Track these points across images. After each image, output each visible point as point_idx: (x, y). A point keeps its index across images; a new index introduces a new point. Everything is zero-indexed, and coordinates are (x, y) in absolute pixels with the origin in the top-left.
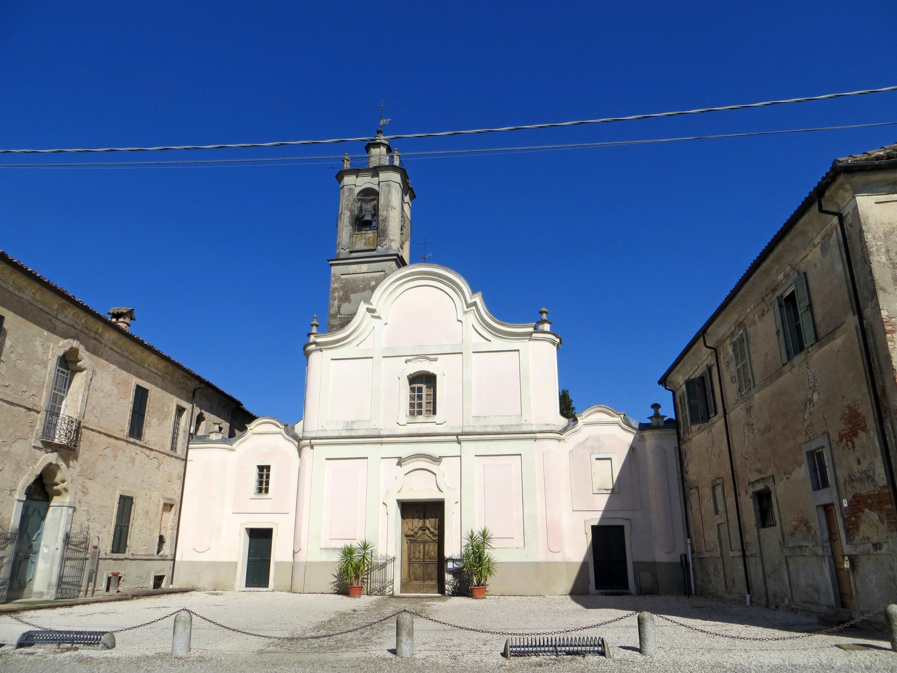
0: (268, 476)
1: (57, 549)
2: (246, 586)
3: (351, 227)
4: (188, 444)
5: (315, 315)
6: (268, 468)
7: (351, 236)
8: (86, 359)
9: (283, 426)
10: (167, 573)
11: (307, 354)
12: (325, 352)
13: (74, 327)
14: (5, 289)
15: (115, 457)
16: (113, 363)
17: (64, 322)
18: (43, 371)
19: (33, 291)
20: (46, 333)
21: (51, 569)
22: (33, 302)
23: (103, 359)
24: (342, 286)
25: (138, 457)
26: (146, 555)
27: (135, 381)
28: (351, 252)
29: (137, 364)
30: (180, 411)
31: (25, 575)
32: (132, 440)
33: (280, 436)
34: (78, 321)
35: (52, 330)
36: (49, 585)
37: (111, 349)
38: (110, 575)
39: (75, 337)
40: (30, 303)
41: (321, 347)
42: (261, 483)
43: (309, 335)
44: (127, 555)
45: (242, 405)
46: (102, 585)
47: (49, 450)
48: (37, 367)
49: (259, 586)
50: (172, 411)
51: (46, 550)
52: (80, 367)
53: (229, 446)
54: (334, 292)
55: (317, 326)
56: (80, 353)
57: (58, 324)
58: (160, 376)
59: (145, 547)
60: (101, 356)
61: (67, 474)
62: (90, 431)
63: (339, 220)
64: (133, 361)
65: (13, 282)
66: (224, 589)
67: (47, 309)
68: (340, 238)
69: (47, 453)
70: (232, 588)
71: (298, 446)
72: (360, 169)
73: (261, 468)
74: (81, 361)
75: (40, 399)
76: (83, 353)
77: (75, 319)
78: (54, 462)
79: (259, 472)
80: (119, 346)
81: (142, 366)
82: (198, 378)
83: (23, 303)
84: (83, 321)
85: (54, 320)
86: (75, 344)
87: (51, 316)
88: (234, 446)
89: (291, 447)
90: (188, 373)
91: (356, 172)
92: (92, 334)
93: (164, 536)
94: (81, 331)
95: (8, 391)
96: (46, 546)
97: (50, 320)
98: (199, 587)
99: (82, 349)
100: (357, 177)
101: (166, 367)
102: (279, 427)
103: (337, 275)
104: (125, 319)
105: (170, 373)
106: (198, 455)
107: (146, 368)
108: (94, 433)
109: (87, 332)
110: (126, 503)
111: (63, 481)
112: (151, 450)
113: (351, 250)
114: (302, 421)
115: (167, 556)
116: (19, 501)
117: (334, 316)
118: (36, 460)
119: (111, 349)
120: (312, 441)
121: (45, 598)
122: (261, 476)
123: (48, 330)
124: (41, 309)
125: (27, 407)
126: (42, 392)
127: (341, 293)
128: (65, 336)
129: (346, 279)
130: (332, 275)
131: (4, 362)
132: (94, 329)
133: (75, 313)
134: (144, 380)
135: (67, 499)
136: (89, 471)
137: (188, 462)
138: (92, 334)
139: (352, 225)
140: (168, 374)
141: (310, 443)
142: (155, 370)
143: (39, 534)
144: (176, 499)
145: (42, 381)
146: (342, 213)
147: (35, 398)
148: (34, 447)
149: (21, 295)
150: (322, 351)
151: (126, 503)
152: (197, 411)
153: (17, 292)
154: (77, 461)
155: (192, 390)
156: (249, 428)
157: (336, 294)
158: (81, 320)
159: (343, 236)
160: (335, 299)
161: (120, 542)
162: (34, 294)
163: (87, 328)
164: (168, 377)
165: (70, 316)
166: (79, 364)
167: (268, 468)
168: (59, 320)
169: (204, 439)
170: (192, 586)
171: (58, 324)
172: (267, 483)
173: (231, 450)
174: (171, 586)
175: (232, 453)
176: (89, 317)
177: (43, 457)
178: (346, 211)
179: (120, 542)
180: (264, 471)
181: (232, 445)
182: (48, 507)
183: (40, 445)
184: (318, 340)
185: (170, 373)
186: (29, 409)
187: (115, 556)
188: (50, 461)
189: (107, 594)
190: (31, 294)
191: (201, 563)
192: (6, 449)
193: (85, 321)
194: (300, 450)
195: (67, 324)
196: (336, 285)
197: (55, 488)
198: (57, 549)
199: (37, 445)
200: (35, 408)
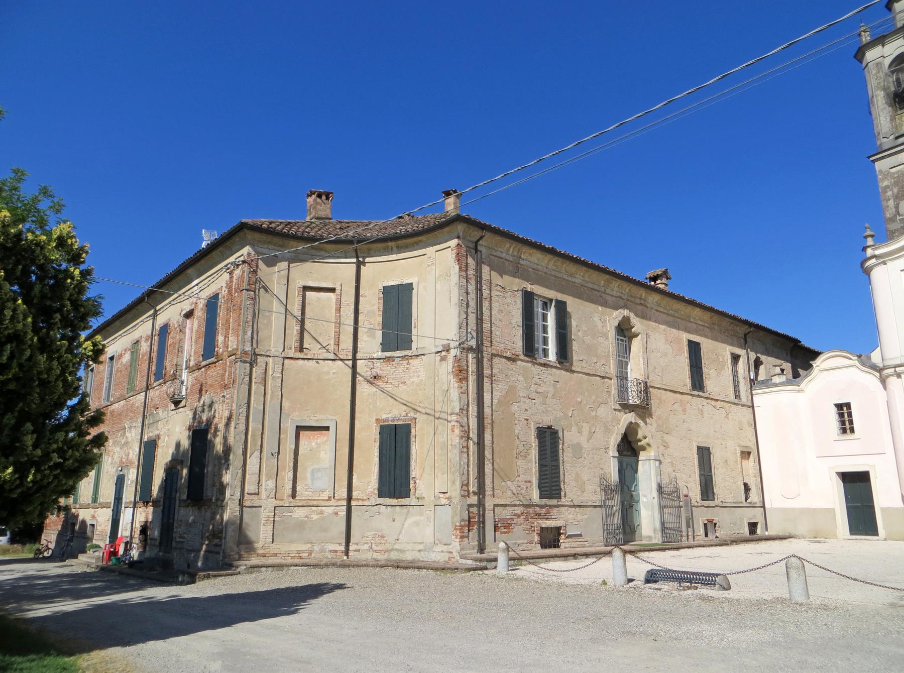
0: (850, 415)
1: (654, 498)
2: (851, 534)
3: (890, 108)
4: (751, 391)
5: (867, 225)
6: (848, 405)
7: (893, 119)
8: (638, 325)
9: (856, 358)
10: (759, 519)
11: (867, 272)
12: (889, 264)
13: (621, 298)
14: (560, 278)
15: (684, 411)
16: (662, 324)
17: (612, 296)
18: (606, 342)
19: (582, 274)
20: (600, 308)
21: (653, 516)
23: (652, 321)
24: (894, 182)
25: (705, 409)
26: (735, 503)
27: (685, 337)
28: (897, 138)
30: (735, 358)
31: (633, 521)
32: (696, 393)
33: (854, 368)
34: (623, 292)
35: (605, 304)
36: (655, 530)
37: (657, 311)
38: (706, 522)
39: (625, 307)
40: (582, 285)
41: (883, 259)
42: (843, 423)
43: (864, 249)
44: (716, 502)
45: (800, 342)
46: (700, 531)
47: (627, 411)
48: (601, 340)
49: (867, 534)
50: (727, 359)
51: (645, 500)
52: (634, 333)
53: (796, 388)
54: (886, 192)
55: (872, 236)
56: (632, 320)
57: (608, 298)
58: (707, 327)
59: (732, 495)
60: (650, 320)
61: (646, 431)
63: (871, 106)
64: (679, 318)
65: (565, 271)
66: (826, 537)
67: (596, 287)
68: (878, 126)
69: (626, 413)
70: (835, 536)
71: (881, 377)
72: (885, 34)
73: (839, 407)
74: (633, 327)
75: (610, 367)
76: (635, 321)
78: (634, 421)
79: (838, 410)
82: (746, 323)
83: (577, 287)
85: (604, 295)
86: (625, 312)
87: (601, 293)
88: (802, 386)
89: (871, 380)
90: (734, 318)
91: (880, 40)
92: (638, 301)
93: (748, 483)
94: (628, 300)
96: (645, 496)
98: (797, 534)
99: (632, 316)
100: (883, 46)
101: (711, 318)
102: (850, 359)
103: (884, 170)
104: (662, 280)
105: (716, 323)
106: (764, 400)
107: (692, 322)
108: (661, 391)
109: (633, 299)
110: (704, 454)
111: (645, 438)
112: (716, 400)
113: (897, 135)
114: (879, 348)
115: (756, 503)
116: (614, 457)
117: (892, 220)
118: (618, 421)
119: (657, 311)
120: (897, 369)
121: (654, 542)
122: (841, 415)
124: (592, 289)
125: (601, 375)
126: (610, 361)
127: (895, 190)
129: (898, 172)
130: (877, 173)
131: (575, 340)
132: (638, 296)
133: (619, 285)
134: (693, 334)
135: (650, 453)
136: (665, 427)
137: (755, 408)
138: (638, 301)
139: (890, 105)
140: (715, 324)
141: (895, 371)
142: (701, 323)
143: (636, 485)
144: (752, 447)
145: (607, 351)
146: (873, 97)
147: (605, 366)
148: (614, 410)
149: (574, 280)
150: (886, 264)
151: (704, 454)
152: (753, 356)
153: (570, 279)
154: (652, 418)
155: (743, 336)
156: (814, 365)
157: (889, 193)
158: (625, 291)
159: (882, 122)
160: (889, 200)
161: (708, 491)
162: (583, 277)
163: (632, 296)
164: (716, 327)
165: (616, 289)
166: (633, 330)
167: (848, 405)
168: (608, 294)
169: (767, 383)
170: (789, 533)
172: (851, 422)
173: (799, 391)
174: (767, 533)
175: (801, 394)
176: (631, 285)
177: (624, 417)
178: (878, 92)
179: (708, 491)
180: (844, 410)
181: (799, 386)
182: (638, 461)
183: (618, 407)
184: (877, 252)
185: (716, 323)
186: (603, 377)
187: (706, 503)
189: (706, 539)
190: (581, 278)
191: (793, 509)
192: (594, 414)
194: (883, 381)
196: (886, 183)
197: (639, 443)
198: (654, 498)
199: (617, 408)
200: (607, 375)
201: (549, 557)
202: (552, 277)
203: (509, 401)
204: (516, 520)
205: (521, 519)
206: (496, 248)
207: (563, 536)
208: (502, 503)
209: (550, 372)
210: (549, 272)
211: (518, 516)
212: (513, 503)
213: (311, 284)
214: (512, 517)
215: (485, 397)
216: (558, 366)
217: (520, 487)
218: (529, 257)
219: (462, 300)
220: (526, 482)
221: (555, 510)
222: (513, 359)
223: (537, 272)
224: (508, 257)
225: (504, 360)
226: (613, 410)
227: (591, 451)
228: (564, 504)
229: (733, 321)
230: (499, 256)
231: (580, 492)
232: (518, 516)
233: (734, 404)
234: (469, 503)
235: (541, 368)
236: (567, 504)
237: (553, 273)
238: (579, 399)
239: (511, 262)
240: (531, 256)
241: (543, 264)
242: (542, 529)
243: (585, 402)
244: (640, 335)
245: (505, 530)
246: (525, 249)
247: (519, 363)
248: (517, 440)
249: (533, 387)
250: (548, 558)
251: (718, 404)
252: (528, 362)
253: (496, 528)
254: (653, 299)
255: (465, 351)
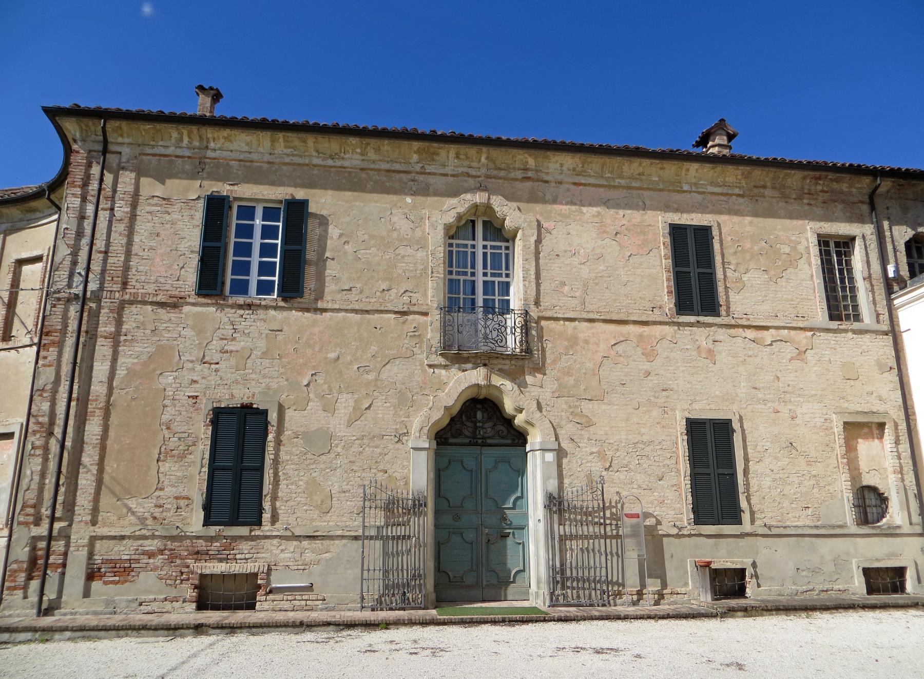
13: (468, 175)
14: (307, 165)
20: (409, 200)
22: (366, 165)
23: (561, 204)
29: (661, 190)
31: (505, 564)
34: (475, 164)
39: (481, 188)
40: (362, 169)
46: (686, 584)
47: (469, 366)
50: (808, 248)
58: (738, 195)
59: (810, 511)
62: (562, 322)
65: (317, 151)
74: (505, 219)
75: (425, 295)
76: (500, 205)
77: (466, 163)
80: (592, 174)
81: (678, 191)
83: (350, 173)
84: (483, 159)
85: (421, 178)
87: (413, 174)
93: (879, 487)
95: (353, 296)
97: (413, 180)
104: (713, 141)
105: (769, 184)
107: (686, 191)
109: (502, 173)
115: (899, 527)
118: (442, 385)
123: (414, 194)
124: (388, 171)
125: (396, 310)
128: (454, 193)
131: (333, 259)
136: (583, 387)
140: (764, 187)
147: (411, 295)
153: (330, 162)
154: (545, 374)
162: (362, 154)
171: (432, 180)
185: (769, 184)
188: (474, 381)
193: (487, 158)
195: (453, 176)
201: (127, 629)
202: (285, 168)
203: (154, 371)
204: (145, 561)
205: (159, 560)
206: (152, 143)
207: (261, 592)
208: (113, 534)
209: (262, 316)
210: (278, 160)
211: (151, 555)
212: (137, 533)
213: (25, 255)
214: (136, 557)
215: (95, 368)
216: (282, 304)
217: (160, 506)
218: (227, 144)
219: (67, 229)
220: (177, 498)
221: (245, 546)
222: (174, 304)
223: (248, 164)
224: (179, 152)
225: (149, 308)
226: (427, 368)
227: (357, 442)
228: (268, 534)
229: (817, 174)
230: (161, 153)
231: (317, 512)
232: (151, 555)
233: (828, 330)
234: (33, 534)
235: (241, 312)
236: (274, 534)
237: (287, 160)
238: (332, 355)
239: (189, 157)
240: (231, 141)
241: (260, 149)
242: (203, 576)
243: (349, 358)
244: (520, 231)
245: (117, 578)
246: (209, 132)
247: (186, 309)
248: (166, 432)
249: (216, 344)
250: (122, 629)
251: (768, 336)
252: (208, 305)
253: (91, 576)
254: (562, 165)
255: (61, 302)
